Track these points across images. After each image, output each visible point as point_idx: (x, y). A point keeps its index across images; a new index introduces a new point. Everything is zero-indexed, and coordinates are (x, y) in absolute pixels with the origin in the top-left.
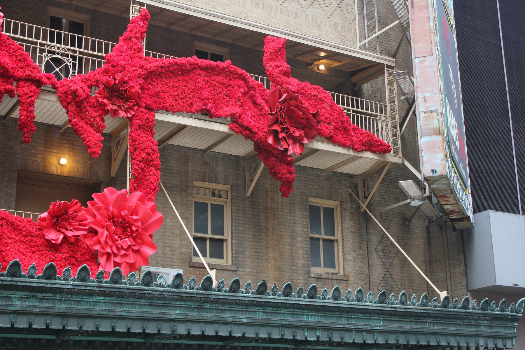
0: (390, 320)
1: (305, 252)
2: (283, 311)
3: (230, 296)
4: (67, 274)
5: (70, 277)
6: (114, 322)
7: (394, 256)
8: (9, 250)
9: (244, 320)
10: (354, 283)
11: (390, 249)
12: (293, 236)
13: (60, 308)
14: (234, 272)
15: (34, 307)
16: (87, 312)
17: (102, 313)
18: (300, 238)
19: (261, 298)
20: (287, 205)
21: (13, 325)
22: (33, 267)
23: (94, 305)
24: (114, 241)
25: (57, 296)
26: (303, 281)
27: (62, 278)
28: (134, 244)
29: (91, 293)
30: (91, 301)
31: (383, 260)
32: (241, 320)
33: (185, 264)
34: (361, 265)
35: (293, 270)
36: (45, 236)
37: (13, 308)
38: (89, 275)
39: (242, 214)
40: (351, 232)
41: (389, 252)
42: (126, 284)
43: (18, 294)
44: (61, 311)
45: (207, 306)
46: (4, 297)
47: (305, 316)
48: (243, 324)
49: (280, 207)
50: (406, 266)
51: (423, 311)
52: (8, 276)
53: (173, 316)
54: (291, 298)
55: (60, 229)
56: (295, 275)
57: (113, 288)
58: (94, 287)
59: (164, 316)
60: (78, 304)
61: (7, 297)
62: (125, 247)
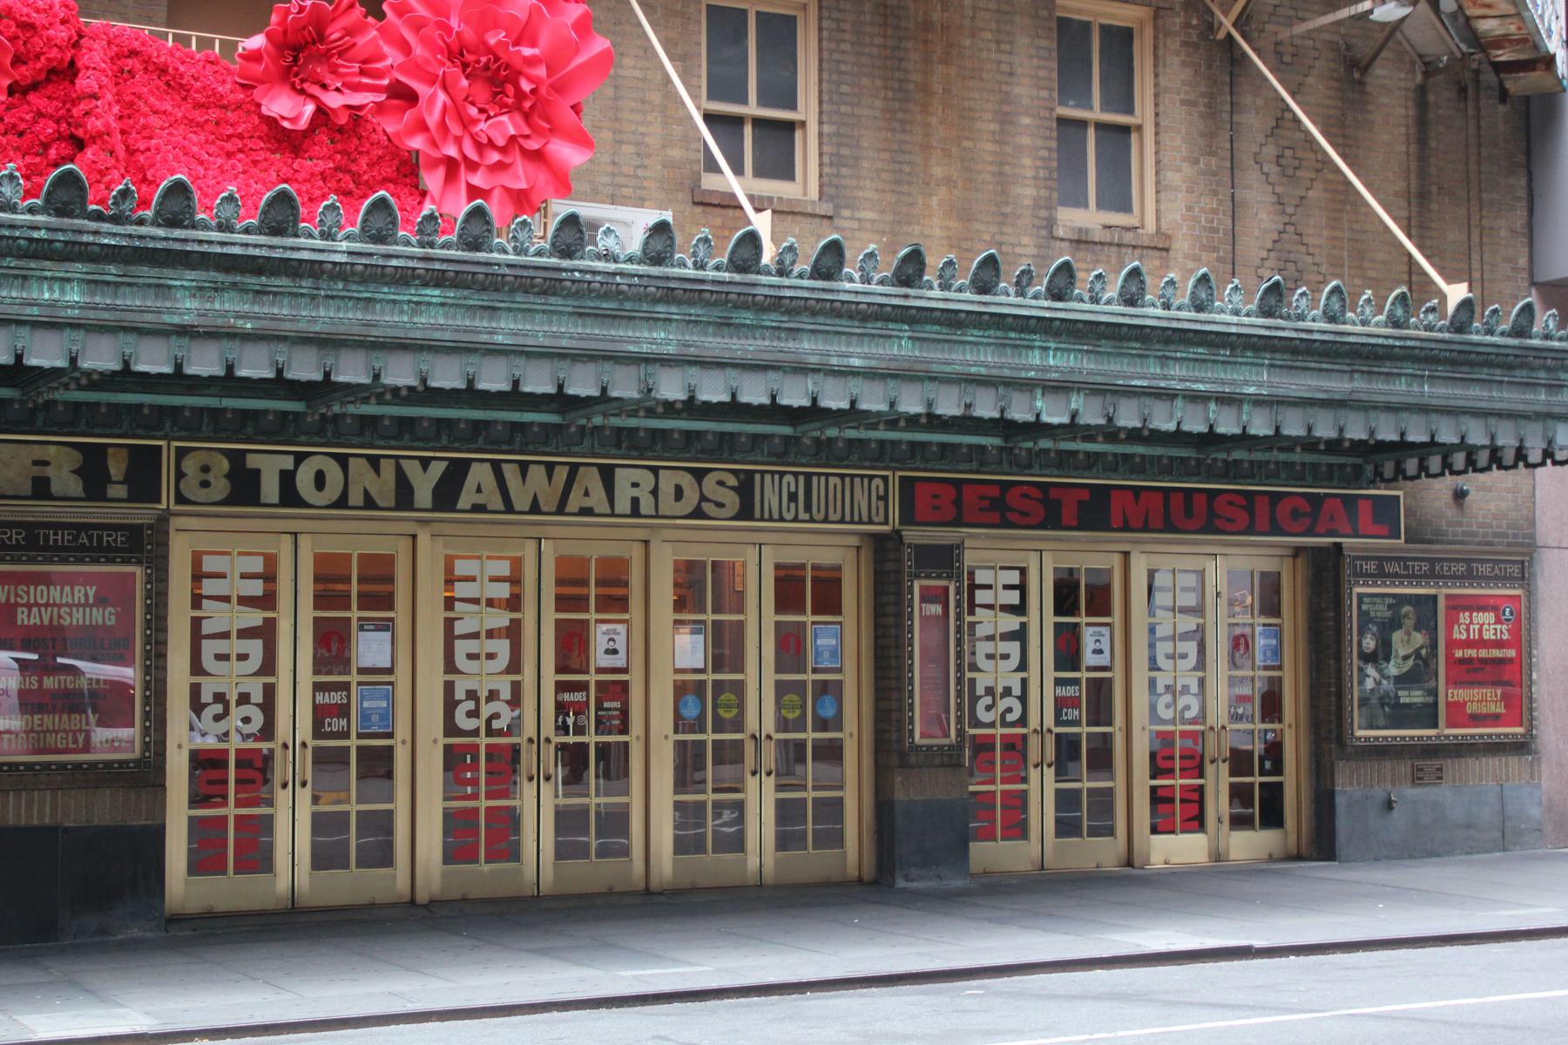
0: (1291, 367)
1: (1039, 163)
2: (973, 335)
3: (813, 289)
4: (330, 219)
5: (341, 228)
6: (473, 363)
7: (1313, 176)
8: (158, 149)
9: (856, 362)
10: (1186, 256)
11: (1300, 154)
12: (1008, 114)
13: (314, 320)
14: (826, 222)
15: (238, 316)
16: (391, 332)
17: (437, 335)
18: (1026, 121)
19: (906, 296)
20: (988, 15)
21: (179, 367)
22: (231, 199)
23: (414, 313)
24: (467, 123)
25: (304, 284)
26: (1031, 251)
27: (316, 232)
28: (527, 131)
29: (403, 278)
30: (402, 302)
31: (1278, 190)
32: (845, 361)
33: (680, 196)
34: (1208, 202)
35: (1004, 215)
36: (259, 106)
37: (176, 320)
38: (394, 223)
39: (853, 44)
40: (1183, 102)
41: (1296, 163)
42: (505, 252)
43: (190, 277)
44: (318, 329)
45: (747, 317)
46: (150, 286)
47: (1037, 352)
48: (853, 373)
49: (967, 23)
50: (1348, 208)
51: (1391, 342)
52: (159, 225)
53: (645, 348)
54: (997, 299)
55: (306, 86)
56: (1009, 230)
57: (465, 262)
58: (412, 258)
59: (619, 347)
60: (366, 310)
61: (158, 286)
62: (501, 142)
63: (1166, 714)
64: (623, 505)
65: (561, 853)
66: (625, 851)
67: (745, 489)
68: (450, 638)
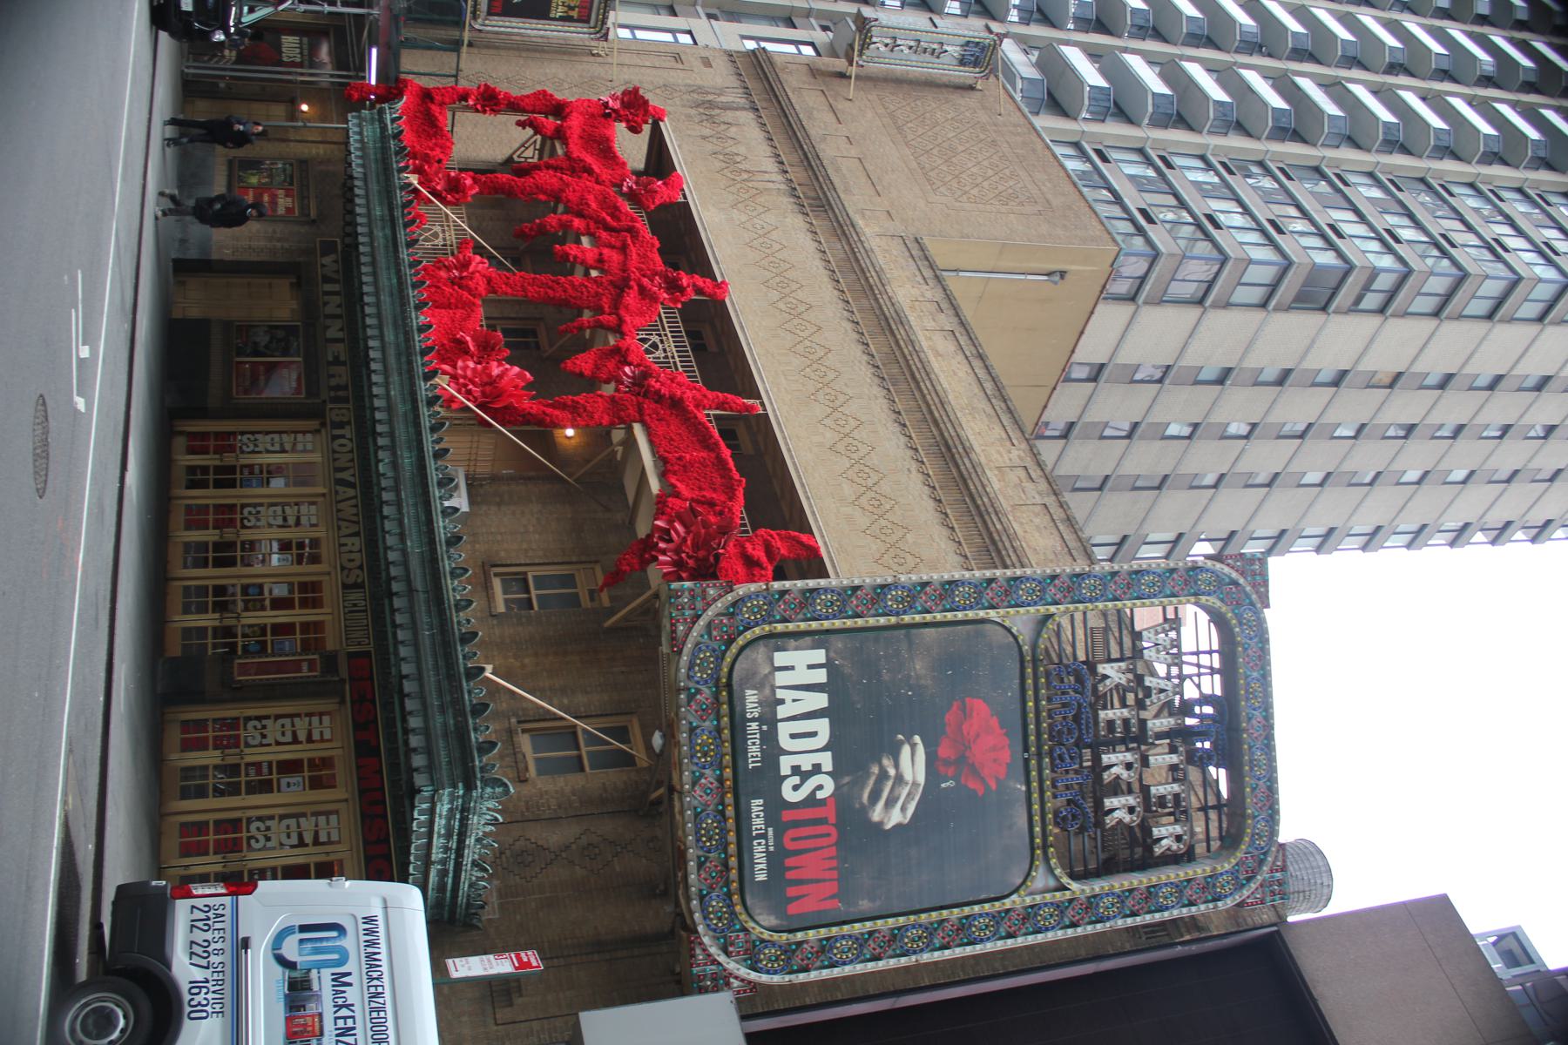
2: (411, 430)
29: (398, 272)
34: (553, 803)
43: (388, 232)
45: (404, 359)
63: (246, 511)
64: (343, 540)
65: (187, 545)
66: (185, 567)
67: (356, 586)
68: (283, 505)
